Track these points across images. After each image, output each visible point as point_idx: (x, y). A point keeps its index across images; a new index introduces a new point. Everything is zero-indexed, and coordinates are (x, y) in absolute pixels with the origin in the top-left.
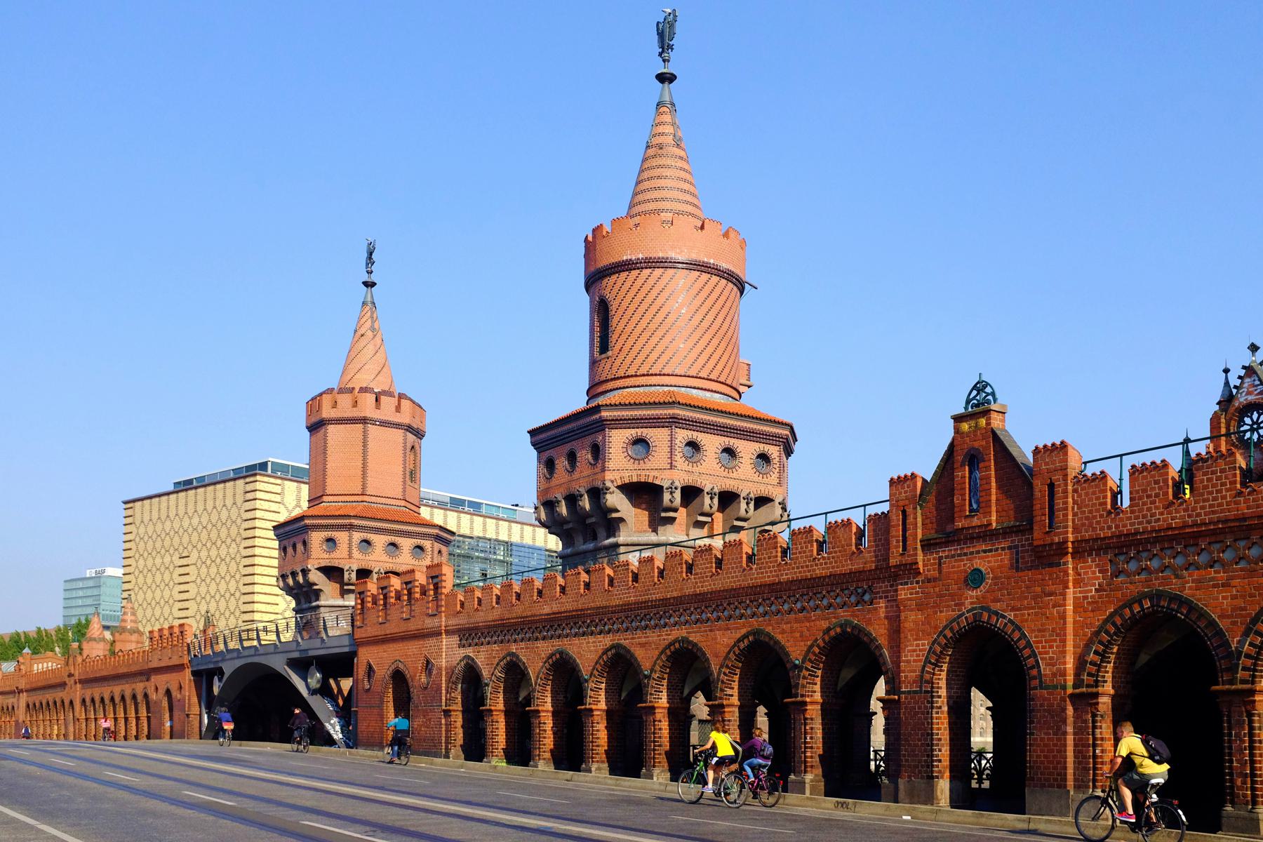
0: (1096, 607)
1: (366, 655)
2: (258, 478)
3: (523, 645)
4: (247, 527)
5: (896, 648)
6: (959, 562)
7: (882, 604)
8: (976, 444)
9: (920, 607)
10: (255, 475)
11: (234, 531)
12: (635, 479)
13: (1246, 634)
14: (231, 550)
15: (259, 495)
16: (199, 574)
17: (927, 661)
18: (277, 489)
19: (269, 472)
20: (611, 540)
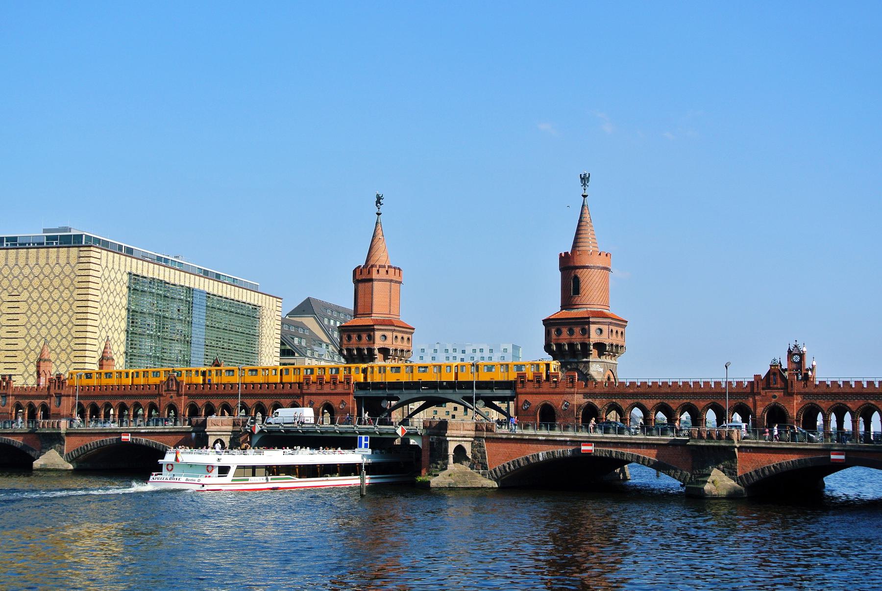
0: (800, 404)
1: (522, 398)
2: (92, 248)
3: (618, 400)
5: (755, 408)
6: (770, 393)
7: (751, 399)
8: (775, 371)
9: (761, 401)
10: (90, 246)
11: (67, 282)
12: (599, 342)
13: (828, 411)
14: (64, 295)
15: (92, 260)
16: (29, 309)
17: (763, 412)
18: (98, 255)
19: (83, 243)
20: (585, 360)
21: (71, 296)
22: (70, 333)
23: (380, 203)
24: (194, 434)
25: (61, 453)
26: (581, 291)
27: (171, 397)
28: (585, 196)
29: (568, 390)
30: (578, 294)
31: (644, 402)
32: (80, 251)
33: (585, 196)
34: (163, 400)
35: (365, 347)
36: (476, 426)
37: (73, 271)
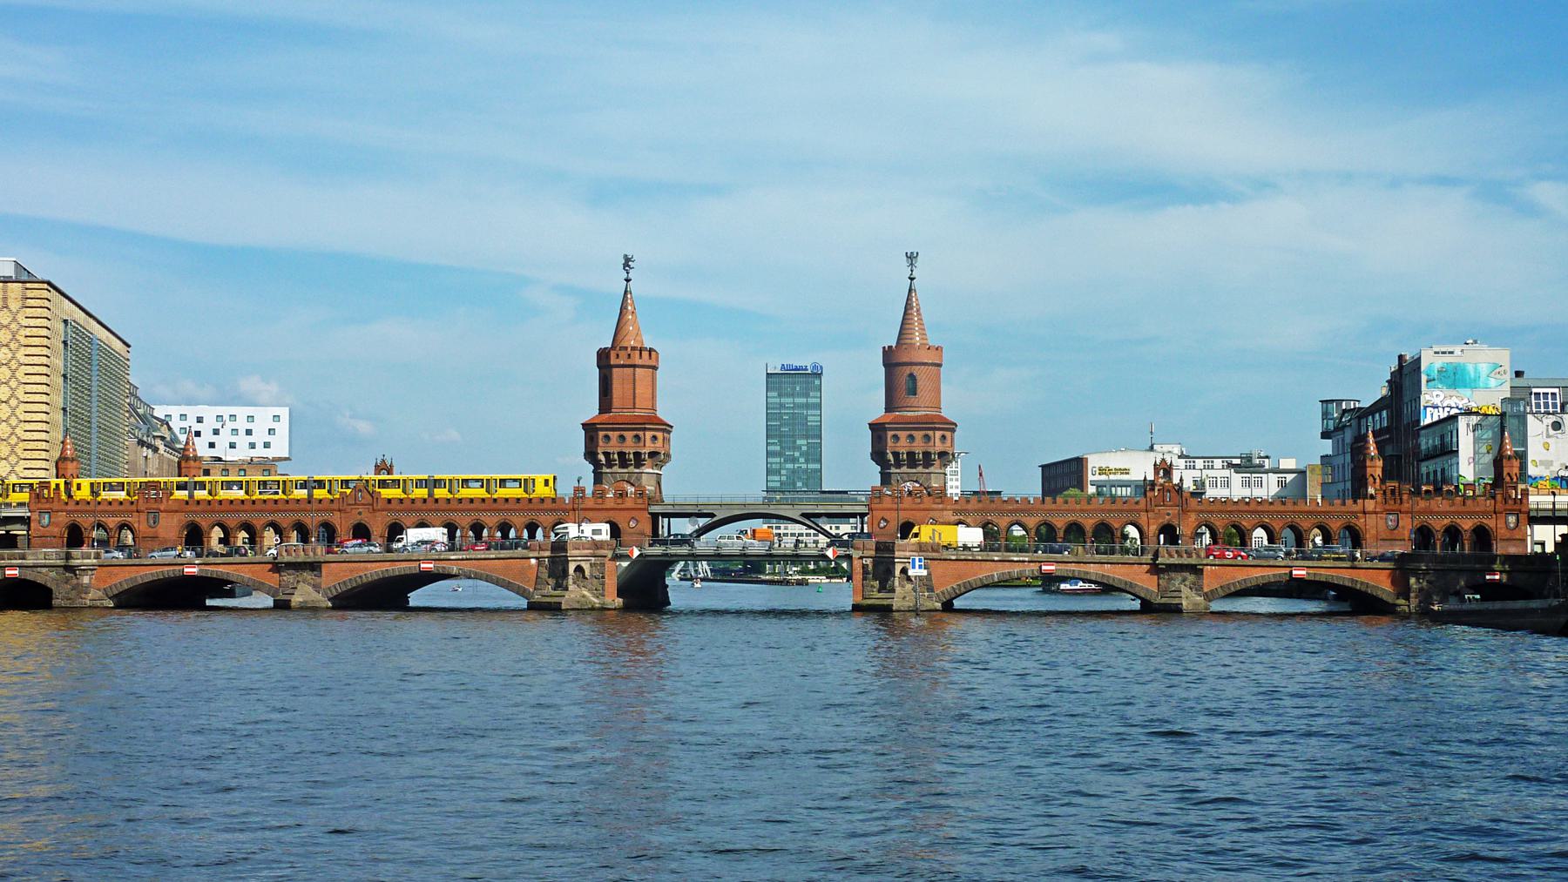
4: (29, 334)
21: (13, 358)
22: (13, 414)
23: (629, 266)
24: (533, 561)
25: (316, 587)
26: (918, 391)
27: (360, 513)
28: (912, 279)
29: (935, 506)
30: (915, 394)
31: (1024, 520)
32: (27, 289)
33: (912, 279)
34: (345, 518)
35: (631, 452)
36: (920, 547)
37: (14, 319)
